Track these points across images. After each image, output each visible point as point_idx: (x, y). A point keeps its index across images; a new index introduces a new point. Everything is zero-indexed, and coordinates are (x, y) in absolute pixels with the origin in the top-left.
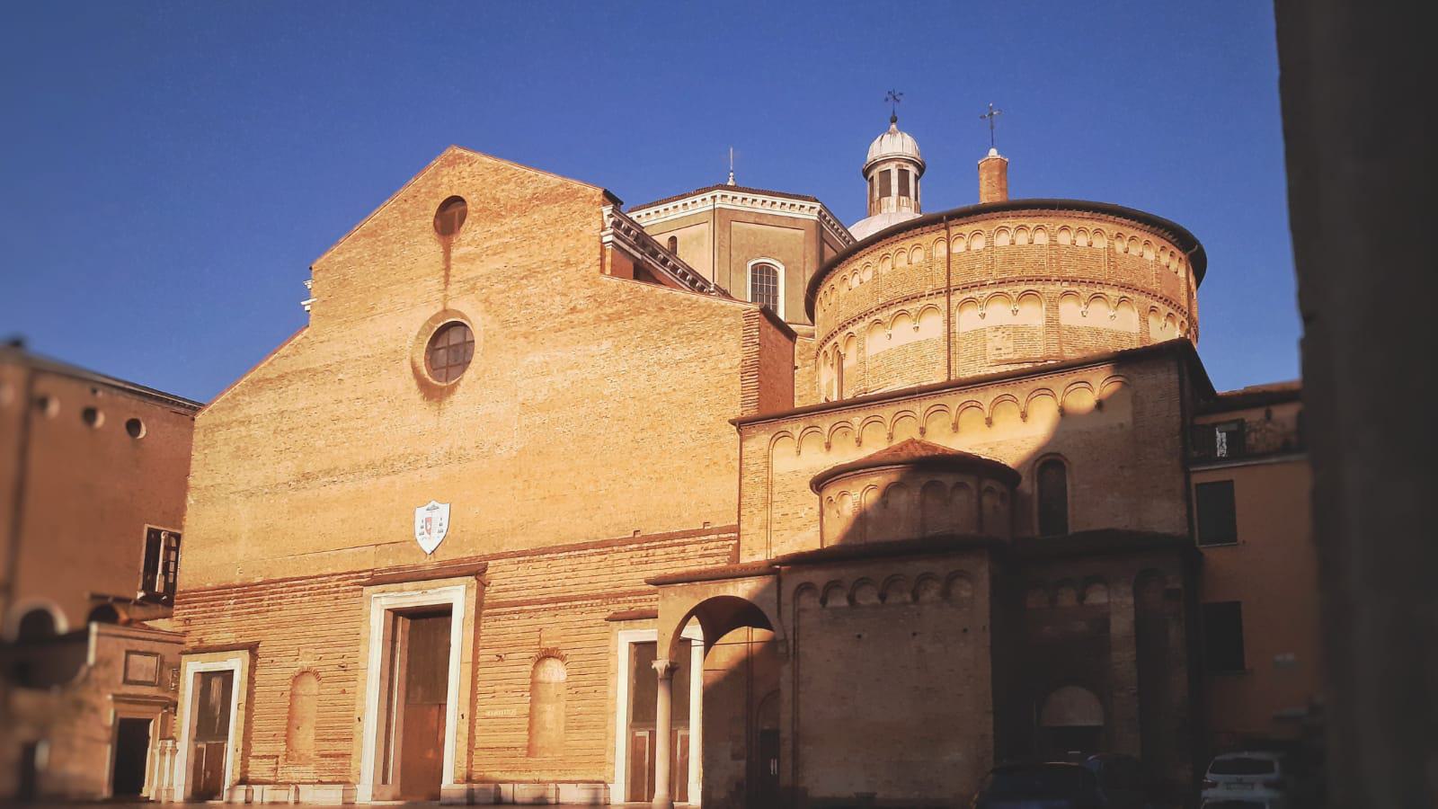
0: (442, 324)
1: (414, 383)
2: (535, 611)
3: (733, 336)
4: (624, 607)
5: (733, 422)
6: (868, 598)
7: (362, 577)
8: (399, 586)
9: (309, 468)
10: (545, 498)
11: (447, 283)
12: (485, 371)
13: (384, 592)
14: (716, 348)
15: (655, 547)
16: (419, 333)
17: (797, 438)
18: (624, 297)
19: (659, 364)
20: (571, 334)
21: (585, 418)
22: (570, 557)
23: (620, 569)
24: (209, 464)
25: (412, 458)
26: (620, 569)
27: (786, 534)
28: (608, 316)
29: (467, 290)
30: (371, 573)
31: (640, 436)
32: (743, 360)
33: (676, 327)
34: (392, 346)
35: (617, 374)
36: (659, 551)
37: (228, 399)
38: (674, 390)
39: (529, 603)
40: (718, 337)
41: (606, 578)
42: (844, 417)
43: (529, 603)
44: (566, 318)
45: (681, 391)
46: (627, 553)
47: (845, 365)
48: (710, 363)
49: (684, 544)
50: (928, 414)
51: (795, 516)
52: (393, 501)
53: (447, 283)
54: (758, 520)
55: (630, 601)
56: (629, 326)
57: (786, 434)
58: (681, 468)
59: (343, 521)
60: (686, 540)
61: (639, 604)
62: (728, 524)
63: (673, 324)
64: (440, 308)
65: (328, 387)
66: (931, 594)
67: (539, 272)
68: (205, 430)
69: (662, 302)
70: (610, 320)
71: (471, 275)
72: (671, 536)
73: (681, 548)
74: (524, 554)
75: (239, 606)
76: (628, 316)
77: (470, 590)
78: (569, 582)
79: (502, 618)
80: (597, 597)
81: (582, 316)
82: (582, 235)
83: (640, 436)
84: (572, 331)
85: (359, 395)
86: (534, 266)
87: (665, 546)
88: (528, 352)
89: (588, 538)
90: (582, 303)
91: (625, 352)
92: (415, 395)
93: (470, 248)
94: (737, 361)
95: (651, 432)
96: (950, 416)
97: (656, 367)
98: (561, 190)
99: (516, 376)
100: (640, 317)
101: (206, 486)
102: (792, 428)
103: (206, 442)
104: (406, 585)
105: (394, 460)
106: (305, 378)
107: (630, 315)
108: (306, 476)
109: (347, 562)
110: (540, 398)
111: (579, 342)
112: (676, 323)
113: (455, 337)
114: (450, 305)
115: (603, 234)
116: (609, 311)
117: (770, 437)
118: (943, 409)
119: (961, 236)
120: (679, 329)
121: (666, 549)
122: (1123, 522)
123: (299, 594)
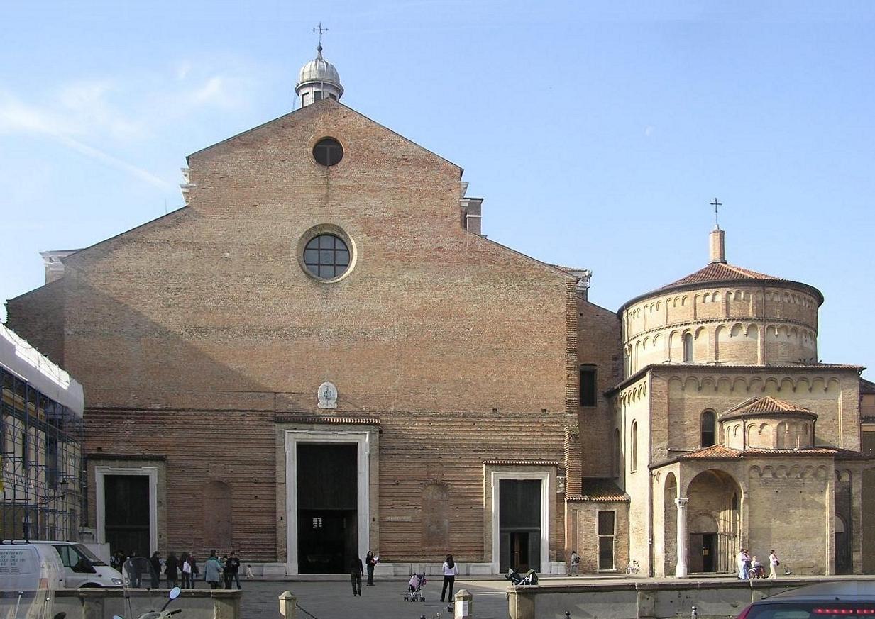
0: (319, 232)
6: (782, 475)
8: (309, 426)
9: (202, 322)
13: (295, 429)
14: (547, 299)
16: (303, 236)
24: (86, 302)
38: (519, 320)
42: (710, 375)
48: (544, 308)
58: (525, 372)
69: (509, 260)
70: (469, 262)
77: (373, 436)
90: (447, 246)
97: (506, 303)
104: (315, 426)
108: (198, 330)
113: (327, 243)
118: (759, 379)
119: (769, 292)
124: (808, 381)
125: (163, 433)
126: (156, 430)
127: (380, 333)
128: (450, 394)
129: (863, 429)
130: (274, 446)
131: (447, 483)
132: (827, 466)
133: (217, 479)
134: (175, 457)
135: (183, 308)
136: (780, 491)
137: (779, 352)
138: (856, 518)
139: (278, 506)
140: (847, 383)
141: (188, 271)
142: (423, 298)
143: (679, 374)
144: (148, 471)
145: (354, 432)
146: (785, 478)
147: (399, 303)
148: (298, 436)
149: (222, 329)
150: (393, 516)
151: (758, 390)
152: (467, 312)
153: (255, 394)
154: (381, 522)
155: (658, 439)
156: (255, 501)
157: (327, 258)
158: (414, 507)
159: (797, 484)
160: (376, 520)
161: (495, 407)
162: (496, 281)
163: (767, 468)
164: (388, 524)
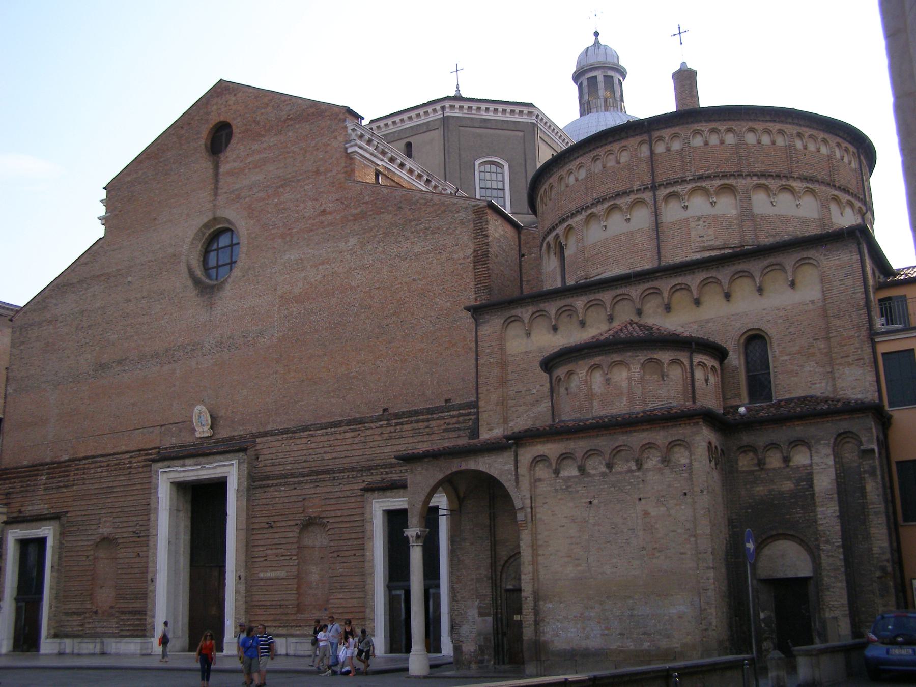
0: (212, 230)
1: (190, 283)
2: (299, 483)
3: (465, 230)
4: (374, 478)
5: (468, 309)
6: (596, 466)
7: (151, 454)
8: (181, 462)
10: (303, 381)
11: (216, 195)
12: (249, 269)
13: (169, 467)
15: (402, 424)
16: (194, 239)
17: (526, 321)
18: (367, 198)
19: (400, 257)
20: (322, 233)
21: (336, 306)
22: (327, 434)
23: (372, 444)
25: (189, 348)
26: (372, 444)
27: (521, 409)
28: (354, 216)
29: (233, 200)
30: (157, 450)
31: (385, 322)
32: (475, 251)
33: (413, 223)
34: (171, 250)
35: (363, 267)
36: (406, 427)
37: (38, 302)
38: (414, 280)
39: (293, 475)
40: (451, 230)
41: (360, 452)
42: (568, 301)
43: (293, 475)
44: (317, 220)
45: (421, 280)
46: (378, 430)
47: (567, 253)
49: (428, 420)
50: (644, 297)
51: (528, 393)
52: (174, 386)
53: (216, 195)
54: (494, 397)
55: (382, 473)
56: (373, 224)
57: (518, 319)
59: (133, 404)
60: (430, 416)
61: (390, 475)
62: (468, 400)
63: (411, 221)
64: (210, 217)
65: (120, 288)
66: (653, 461)
67: (293, 182)
68: (21, 329)
69: (401, 202)
70: (355, 220)
71: (238, 186)
72: (417, 413)
73: (426, 424)
74: (286, 431)
75: (50, 481)
76: (371, 215)
78: (327, 456)
79: (272, 489)
80: (353, 469)
81: (330, 218)
82: (329, 148)
83: (385, 322)
84: (322, 231)
85: (145, 294)
86: (289, 176)
87: (411, 422)
88: (285, 251)
89: (342, 416)
90: (330, 206)
91: (370, 247)
92: (192, 292)
93: (235, 164)
94: (470, 251)
95: (394, 318)
96: (663, 298)
97: (397, 260)
98: (312, 110)
99: (275, 273)
100: (382, 216)
101: (22, 377)
102: (522, 313)
103: (22, 339)
104: (188, 461)
105: (174, 350)
106: (100, 281)
107: (373, 214)
108: (103, 366)
109: (137, 441)
110: (296, 290)
111: (328, 240)
112: (414, 220)
113: (224, 241)
114: (220, 213)
115: (347, 145)
116: (354, 211)
117: (502, 321)
118: (657, 292)
120: (417, 225)
121: (412, 425)
122: (820, 389)
123: (99, 470)
124: (751, 276)
125: (65, 487)
126: (61, 484)
127: (261, 334)
128: (333, 397)
129: (882, 349)
130: (149, 489)
131: (325, 521)
132: (687, 439)
133: (106, 535)
134: (74, 514)
135: (92, 346)
136: (595, 502)
137: (693, 233)
138: (827, 542)
139: (150, 565)
140: (837, 262)
141: (98, 305)
142: (305, 278)
143: (518, 312)
144: (47, 532)
145: (221, 464)
146: (603, 475)
147: (279, 292)
148: (172, 475)
149: (120, 362)
150: (267, 572)
151: (659, 311)
152: (353, 284)
153: (145, 430)
154: (249, 581)
155: (488, 424)
156: (137, 560)
157: (224, 258)
158: (288, 558)
159: (631, 484)
160: (243, 578)
161: (385, 406)
162: (386, 234)
163: (564, 457)
164: (261, 583)
